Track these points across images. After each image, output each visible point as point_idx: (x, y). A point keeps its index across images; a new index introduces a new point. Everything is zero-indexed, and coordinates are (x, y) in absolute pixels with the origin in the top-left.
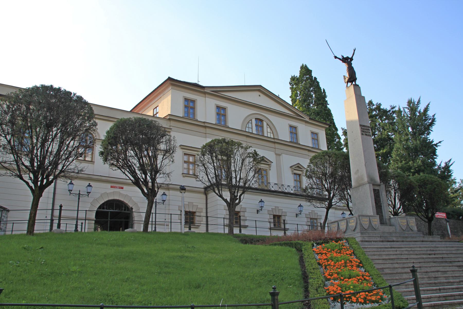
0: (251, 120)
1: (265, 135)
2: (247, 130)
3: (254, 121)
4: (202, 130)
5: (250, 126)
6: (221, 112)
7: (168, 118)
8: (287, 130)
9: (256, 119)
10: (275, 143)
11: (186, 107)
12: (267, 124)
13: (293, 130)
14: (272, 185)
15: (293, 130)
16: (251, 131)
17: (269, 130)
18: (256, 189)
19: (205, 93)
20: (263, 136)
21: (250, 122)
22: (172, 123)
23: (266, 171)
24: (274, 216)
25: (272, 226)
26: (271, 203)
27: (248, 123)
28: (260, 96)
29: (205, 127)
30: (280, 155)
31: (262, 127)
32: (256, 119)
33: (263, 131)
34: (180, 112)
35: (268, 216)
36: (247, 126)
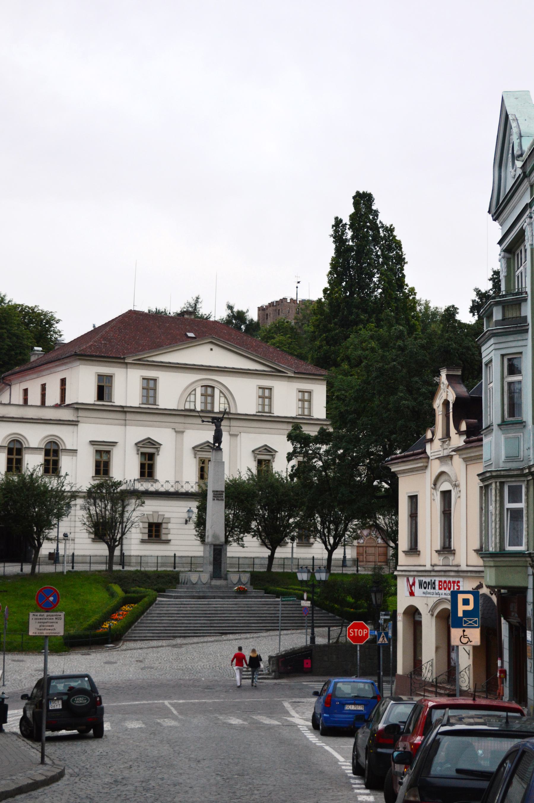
0: (195, 390)
2: (187, 407)
3: (199, 391)
6: (150, 387)
7: (76, 406)
12: (221, 392)
13: (266, 395)
15: (266, 395)
16: (192, 407)
17: (223, 400)
19: (127, 364)
20: (212, 412)
21: (193, 393)
22: (81, 413)
27: (190, 394)
28: (211, 349)
29: (125, 412)
30: (237, 435)
31: (213, 396)
32: (202, 386)
33: (213, 403)
36: (188, 400)
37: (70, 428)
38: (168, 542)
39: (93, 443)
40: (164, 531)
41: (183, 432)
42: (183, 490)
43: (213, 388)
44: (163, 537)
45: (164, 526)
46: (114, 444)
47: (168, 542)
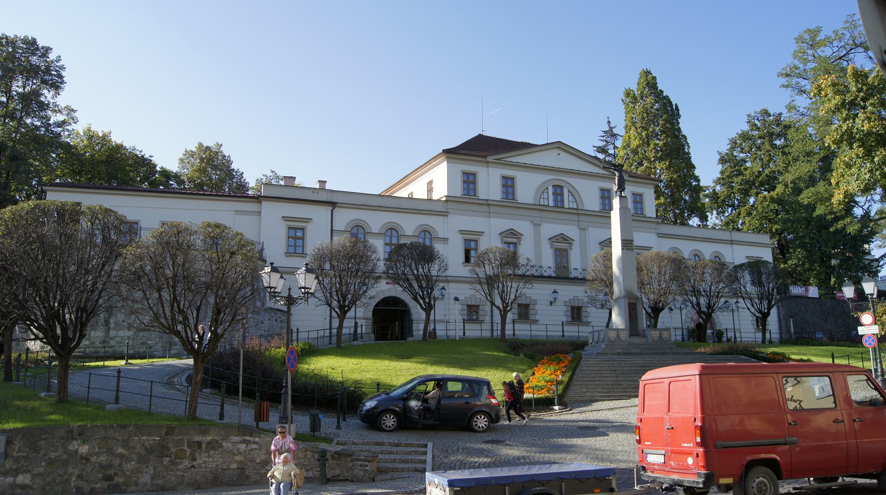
1: (566, 206)
2: (542, 203)
3: (551, 190)
4: (485, 208)
5: (546, 196)
6: (508, 184)
8: (597, 195)
9: (555, 186)
10: (578, 214)
11: (464, 182)
14: (572, 270)
16: (546, 204)
17: (571, 198)
18: (549, 277)
19: (488, 162)
22: (450, 205)
23: (566, 251)
24: (573, 308)
25: (570, 319)
26: (569, 293)
30: (585, 229)
31: (562, 195)
33: (562, 201)
34: (458, 192)
35: (564, 308)
37: (441, 219)
38: (535, 322)
39: (462, 232)
40: (531, 312)
41: (540, 225)
42: (545, 274)
43: (561, 187)
44: (532, 317)
45: (531, 307)
46: (481, 233)
47: (535, 322)
